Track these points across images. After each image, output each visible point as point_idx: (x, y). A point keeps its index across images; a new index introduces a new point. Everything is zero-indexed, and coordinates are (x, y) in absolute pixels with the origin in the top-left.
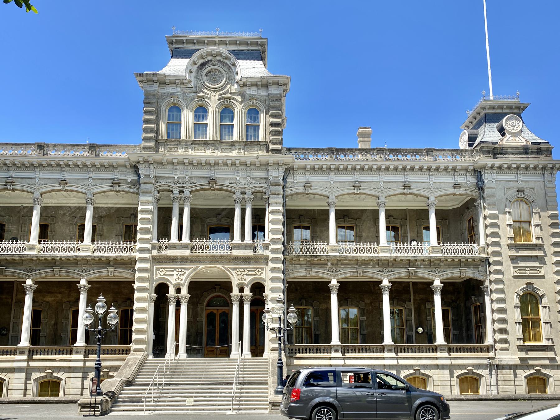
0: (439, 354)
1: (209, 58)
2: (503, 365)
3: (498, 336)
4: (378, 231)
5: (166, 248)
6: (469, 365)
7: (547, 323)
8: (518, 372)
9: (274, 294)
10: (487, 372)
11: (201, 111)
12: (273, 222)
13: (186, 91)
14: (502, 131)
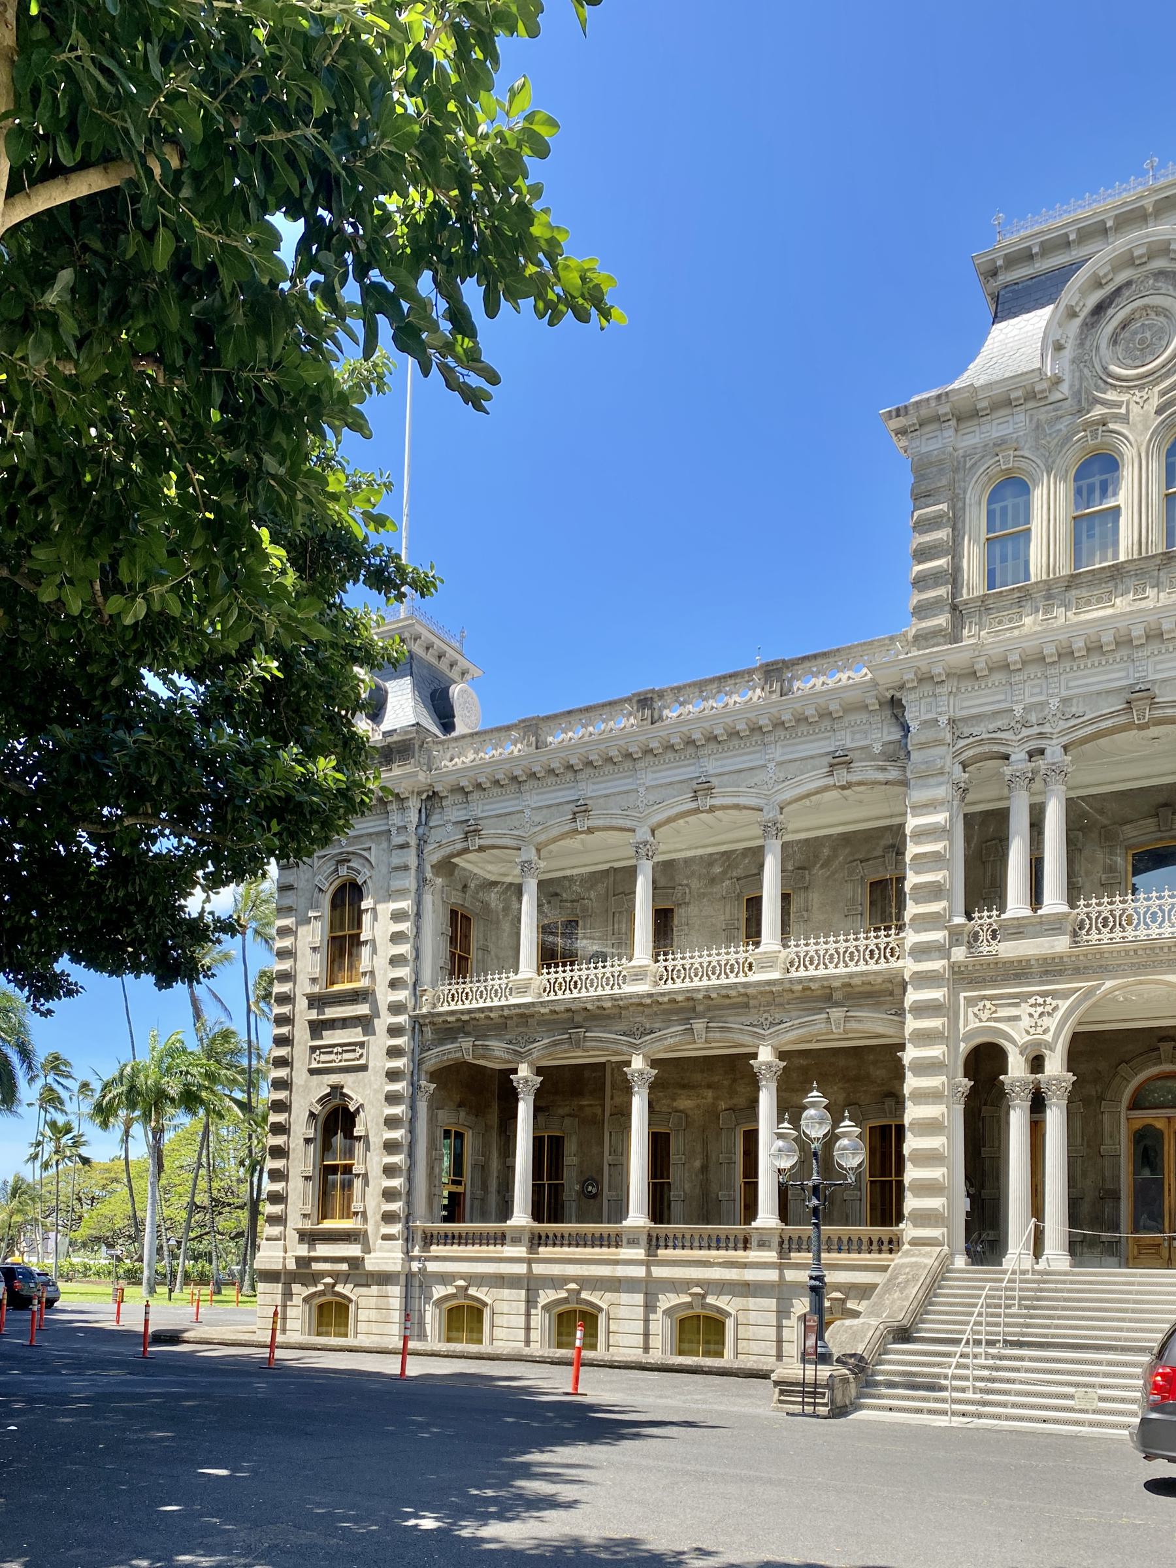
1: (1122, 277)
5: (994, 938)
11: (1098, 470)
13: (1043, 417)
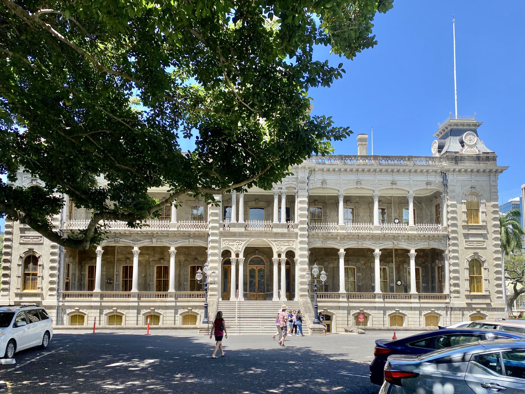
0: (412, 300)
2: (455, 308)
3: (453, 289)
4: (373, 216)
6: (432, 308)
7: (486, 280)
8: (465, 312)
10: (445, 312)
12: (301, 209)
14: (462, 143)
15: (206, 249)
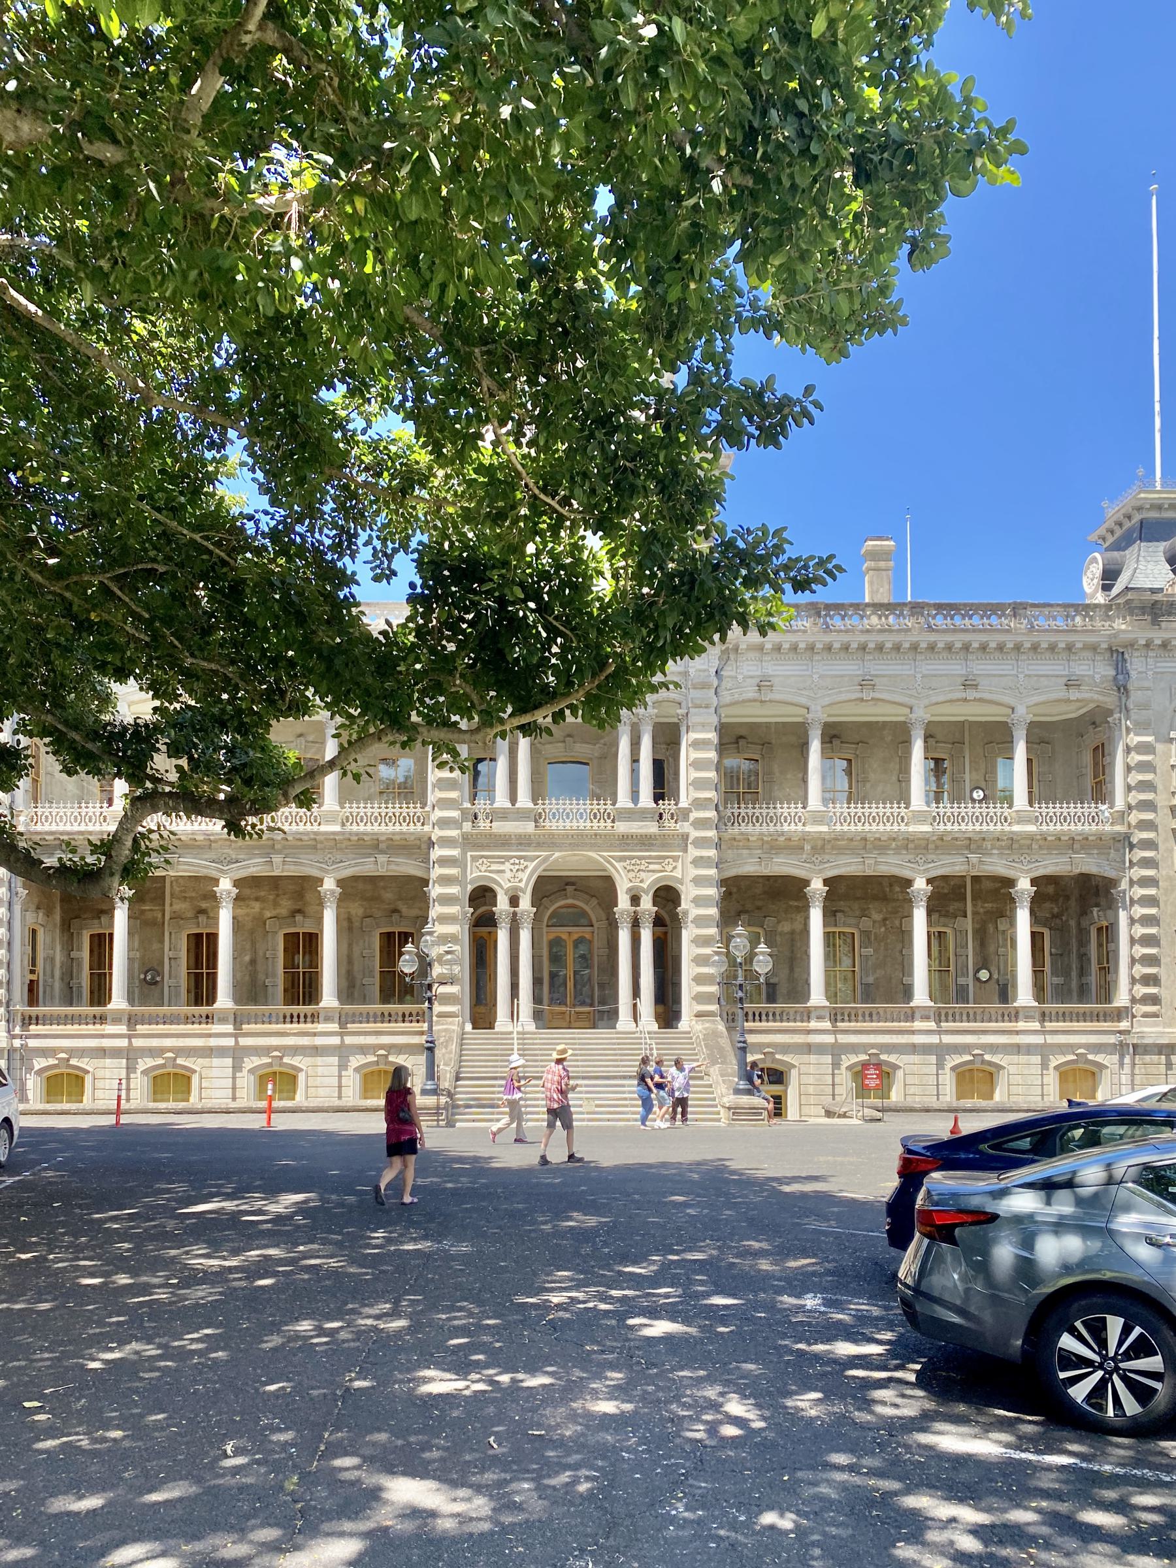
0: (1021, 1025)
2: (1146, 1045)
3: (1141, 990)
6: (1080, 1046)
9: (699, 906)
12: (697, 765)
15: (426, 882)
